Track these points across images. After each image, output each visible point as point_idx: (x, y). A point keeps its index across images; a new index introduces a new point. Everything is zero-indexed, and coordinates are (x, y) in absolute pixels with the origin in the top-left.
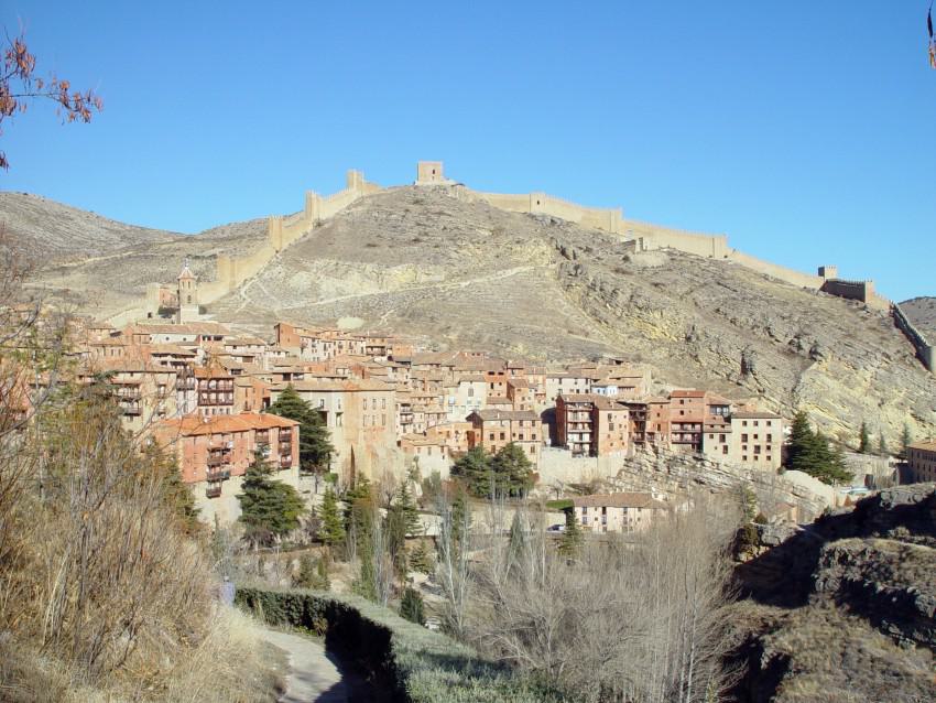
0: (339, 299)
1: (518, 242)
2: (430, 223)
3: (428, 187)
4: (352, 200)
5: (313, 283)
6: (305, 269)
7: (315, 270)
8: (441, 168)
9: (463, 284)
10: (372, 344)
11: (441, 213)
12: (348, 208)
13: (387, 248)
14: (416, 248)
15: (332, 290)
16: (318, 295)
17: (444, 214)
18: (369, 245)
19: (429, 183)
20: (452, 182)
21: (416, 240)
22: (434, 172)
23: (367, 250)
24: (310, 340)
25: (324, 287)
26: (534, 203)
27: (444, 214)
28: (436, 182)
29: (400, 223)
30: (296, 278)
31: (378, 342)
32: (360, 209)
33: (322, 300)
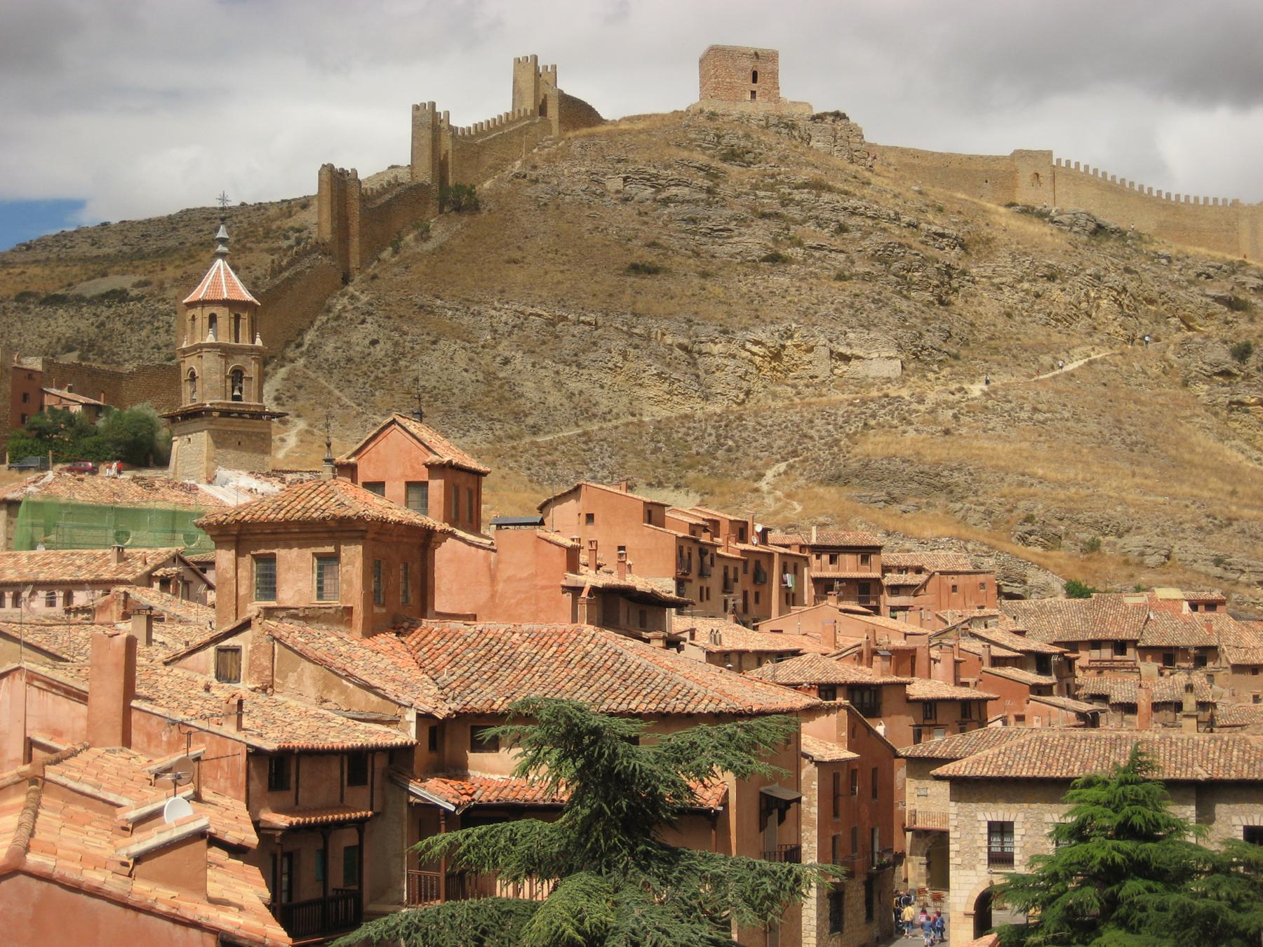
1: (1051, 278)
2: (794, 212)
5: (490, 377)
9: (977, 389)
10: (831, 572)
11: (818, 186)
13: (696, 281)
14: (779, 281)
16: (518, 416)
17: (830, 189)
18: (636, 269)
21: (775, 259)
22: (755, 80)
23: (630, 280)
26: (1025, 177)
27: (830, 189)
29: (700, 211)
31: (849, 567)
33: (535, 430)
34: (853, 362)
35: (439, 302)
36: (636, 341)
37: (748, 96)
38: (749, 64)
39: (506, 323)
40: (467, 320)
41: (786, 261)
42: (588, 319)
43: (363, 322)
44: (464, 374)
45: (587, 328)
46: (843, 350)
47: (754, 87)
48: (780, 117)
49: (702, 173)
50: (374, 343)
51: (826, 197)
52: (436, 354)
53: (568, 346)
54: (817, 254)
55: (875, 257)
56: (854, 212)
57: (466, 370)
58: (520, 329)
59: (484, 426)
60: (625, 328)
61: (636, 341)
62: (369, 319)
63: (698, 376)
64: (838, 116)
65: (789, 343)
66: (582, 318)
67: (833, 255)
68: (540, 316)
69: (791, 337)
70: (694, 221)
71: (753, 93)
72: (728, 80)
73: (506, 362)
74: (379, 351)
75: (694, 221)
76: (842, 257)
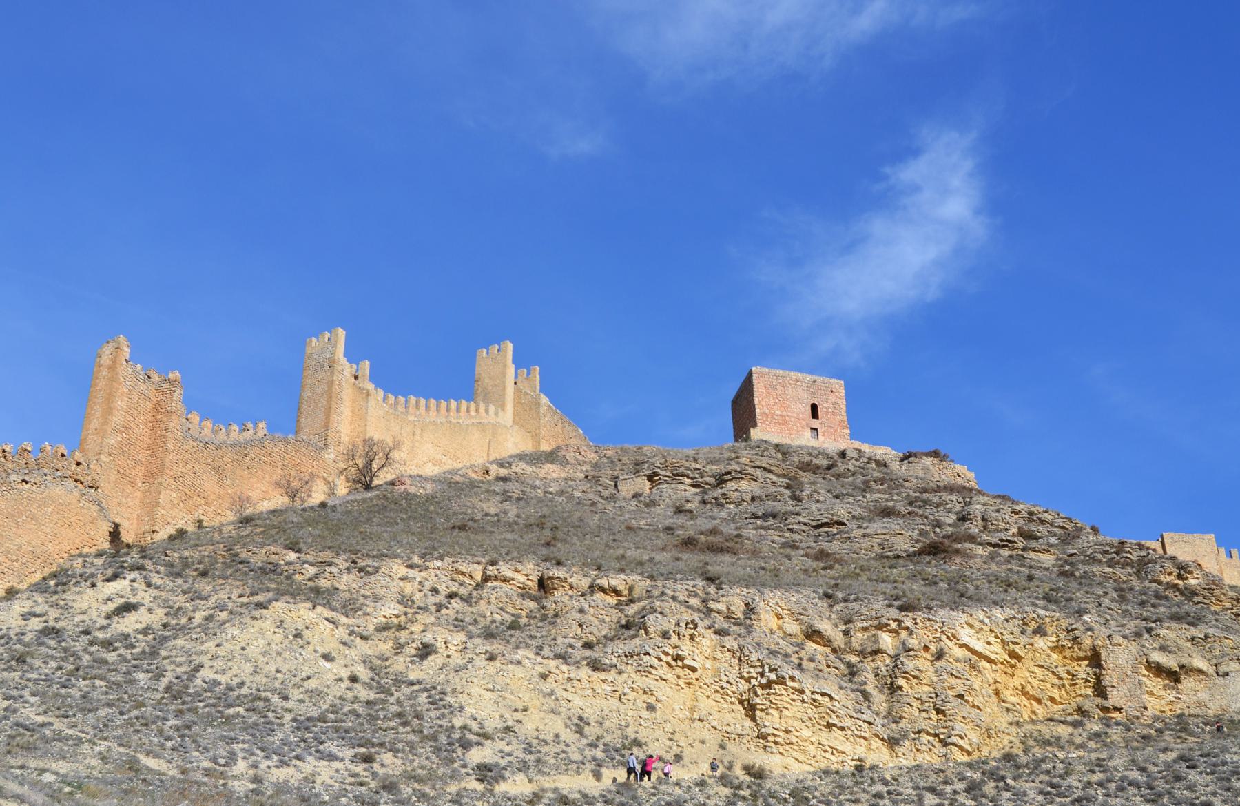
7: (390, 609)
34: (1187, 683)
35: (292, 556)
36: (720, 622)
39: (435, 591)
40: (347, 582)
42: (614, 583)
44: (322, 663)
45: (612, 600)
47: (815, 423)
52: (268, 625)
53: (568, 634)
57: (328, 657)
58: (467, 600)
59: (348, 753)
60: (694, 602)
65: (1040, 643)
68: (505, 580)
72: (778, 412)
73: (426, 651)
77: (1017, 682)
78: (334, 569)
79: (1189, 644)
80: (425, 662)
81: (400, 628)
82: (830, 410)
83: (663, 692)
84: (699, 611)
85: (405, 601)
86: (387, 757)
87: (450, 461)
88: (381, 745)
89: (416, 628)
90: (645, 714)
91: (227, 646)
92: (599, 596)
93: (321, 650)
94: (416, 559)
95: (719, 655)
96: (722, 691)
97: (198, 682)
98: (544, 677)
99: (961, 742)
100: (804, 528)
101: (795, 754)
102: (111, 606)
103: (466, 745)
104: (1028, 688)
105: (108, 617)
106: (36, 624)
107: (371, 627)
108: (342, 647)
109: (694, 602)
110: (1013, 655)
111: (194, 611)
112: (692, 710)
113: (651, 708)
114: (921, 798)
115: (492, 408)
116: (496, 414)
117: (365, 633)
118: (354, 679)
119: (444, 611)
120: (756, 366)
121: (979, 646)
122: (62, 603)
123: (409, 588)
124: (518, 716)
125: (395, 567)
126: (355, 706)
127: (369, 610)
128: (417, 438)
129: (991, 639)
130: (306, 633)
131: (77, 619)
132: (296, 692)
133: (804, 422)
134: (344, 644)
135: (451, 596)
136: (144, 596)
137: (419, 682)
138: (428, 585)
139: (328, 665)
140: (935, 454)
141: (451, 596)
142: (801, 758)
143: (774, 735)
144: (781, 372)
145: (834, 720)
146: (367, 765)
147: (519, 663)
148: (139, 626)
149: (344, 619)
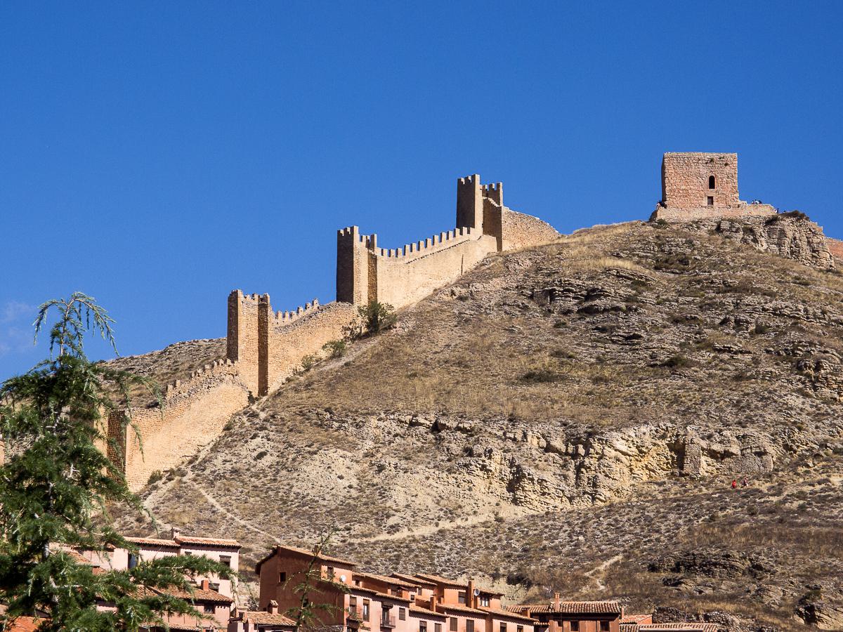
0: (446, 525)
3: (698, 223)
4: (469, 265)
6: (339, 443)
7: (369, 444)
8: (733, 169)
12: (465, 281)
15: (425, 500)
18: (529, 378)
19: (697, 214)
20: (767, 211)
24: (376, 606)
25: (398, 496)
27: (754, 291)
28: (718, 212)
30: (312, 469)
32: (497, 284)
37: (705, 202)
38: (706, 172)
39: (389, 433)
41: (687, 364)
43: (255, 436)
44: (338, 480)
46: (717, 447)
47: (711, 193)
48: (732, 221)
49: (629, 282)
50: (261, 455)
51: (748, 299)
54: (726, 356)
55: (777, 357)
56: (777, 312)
57: (341, 477)
61: (510, 444)
62: (262, 434)
63: (565, 477)
64: (794, 214)
65: (663, 443)
66: (461, 425)
67: (739, 356)
69: (663, 437)
70: (603, 330)
71: (711, 199)
72: (683, 187)
73: (381, 468)
74: (267, 460)
75: (603, 330)
76: (748, 358)
77: (643, 464)
78: (346, 425)
79: (735, 439)
80: (381, 474)
81: (373, 456)
82: (725, 180)
83: (476, 481)
84: (501, 439)
85: (376, 440)
86: (357, 526)
87: (435, 281)
88: (356, 521)
89: (379, 455)
90: (467, 492)
91: (302, 475)
92: (458, 433)
93: (339, 474)
94: (383, 415)
95: (503, 462)
96: (502, 479)
97: (292, 494)
98: (428, 478)
99: (601, 497)
100: (621, 339)
101: (528, 506)
102: (255, 454)
103: (388, 517)
104: (649, 466)
105: (255, 459)
106: (228, 466)
107: (361, 456)
108: (347, 470)
109: (500, 433)
110: (641, 452)
111: (288, 455)
112: (489, 489)
113: (470, 489)
114: (562, 527)
115: (465, 229)
116: (469, 232)
117: (358, 459)
118: (350, 487)
119: (392, 444)
120: (667, 152)
121: (624, 449)
122: (236, 452)
123: (378, 432)
124: (414, 498)
125: (372, 420)
126: (350, 500)
127: (360, 447)
128: (411, 274)
129: (631, 445)
130: (332, 465)
131: (244, 461)
132: (328, 495)
133: (702, 193)
134: (348, 468)
135: (396, 435)
136: (268, 446)
137: (377, 485)
138: (386, 430)
139: (341, 481)
140: (794, 214)
141: (396, 435)
142: (531, 507)
143: (520, 499)
144: (687, 154)
145: (546, 490)
146: (347, 532)
147: (418, 473)
148: (267, 464)
149: (349, 454)
